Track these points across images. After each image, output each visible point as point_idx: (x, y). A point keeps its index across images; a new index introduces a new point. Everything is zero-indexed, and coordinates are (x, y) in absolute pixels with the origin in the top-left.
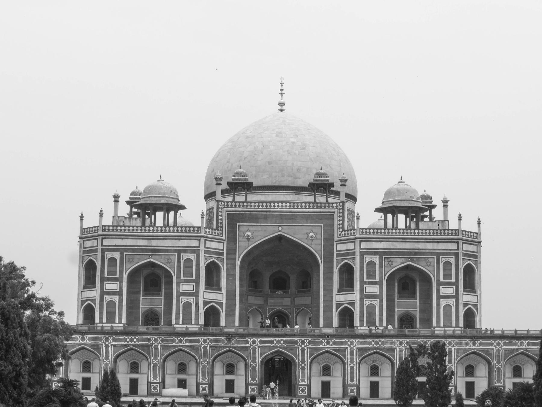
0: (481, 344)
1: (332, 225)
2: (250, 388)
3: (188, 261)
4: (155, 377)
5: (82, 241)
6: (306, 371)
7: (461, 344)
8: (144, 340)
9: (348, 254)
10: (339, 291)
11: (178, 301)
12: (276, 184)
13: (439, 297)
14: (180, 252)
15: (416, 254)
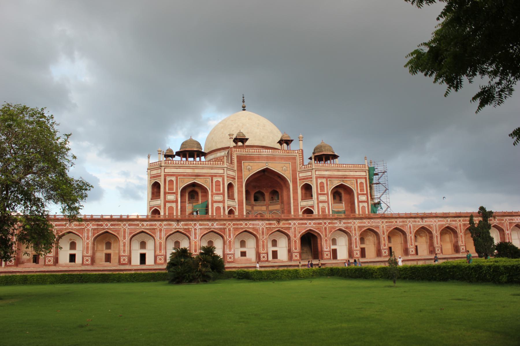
0: (426, 222)
1: (295, 163)
2: (294, 255)
3: (218, 182)
4: (230, 251)
5: (149, 171)
6: (328, 242)
7: (415, 222)
8: (221, 225)
9: (307, 178)
10: (302, 200)
11: (212, 206)
12: (252, 145)
13: (359, 202)
14: (212, 177)
15: (345, 178)
